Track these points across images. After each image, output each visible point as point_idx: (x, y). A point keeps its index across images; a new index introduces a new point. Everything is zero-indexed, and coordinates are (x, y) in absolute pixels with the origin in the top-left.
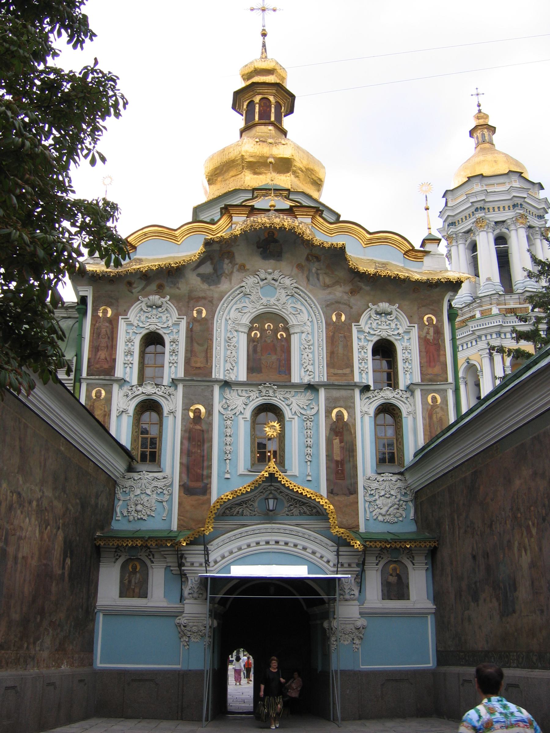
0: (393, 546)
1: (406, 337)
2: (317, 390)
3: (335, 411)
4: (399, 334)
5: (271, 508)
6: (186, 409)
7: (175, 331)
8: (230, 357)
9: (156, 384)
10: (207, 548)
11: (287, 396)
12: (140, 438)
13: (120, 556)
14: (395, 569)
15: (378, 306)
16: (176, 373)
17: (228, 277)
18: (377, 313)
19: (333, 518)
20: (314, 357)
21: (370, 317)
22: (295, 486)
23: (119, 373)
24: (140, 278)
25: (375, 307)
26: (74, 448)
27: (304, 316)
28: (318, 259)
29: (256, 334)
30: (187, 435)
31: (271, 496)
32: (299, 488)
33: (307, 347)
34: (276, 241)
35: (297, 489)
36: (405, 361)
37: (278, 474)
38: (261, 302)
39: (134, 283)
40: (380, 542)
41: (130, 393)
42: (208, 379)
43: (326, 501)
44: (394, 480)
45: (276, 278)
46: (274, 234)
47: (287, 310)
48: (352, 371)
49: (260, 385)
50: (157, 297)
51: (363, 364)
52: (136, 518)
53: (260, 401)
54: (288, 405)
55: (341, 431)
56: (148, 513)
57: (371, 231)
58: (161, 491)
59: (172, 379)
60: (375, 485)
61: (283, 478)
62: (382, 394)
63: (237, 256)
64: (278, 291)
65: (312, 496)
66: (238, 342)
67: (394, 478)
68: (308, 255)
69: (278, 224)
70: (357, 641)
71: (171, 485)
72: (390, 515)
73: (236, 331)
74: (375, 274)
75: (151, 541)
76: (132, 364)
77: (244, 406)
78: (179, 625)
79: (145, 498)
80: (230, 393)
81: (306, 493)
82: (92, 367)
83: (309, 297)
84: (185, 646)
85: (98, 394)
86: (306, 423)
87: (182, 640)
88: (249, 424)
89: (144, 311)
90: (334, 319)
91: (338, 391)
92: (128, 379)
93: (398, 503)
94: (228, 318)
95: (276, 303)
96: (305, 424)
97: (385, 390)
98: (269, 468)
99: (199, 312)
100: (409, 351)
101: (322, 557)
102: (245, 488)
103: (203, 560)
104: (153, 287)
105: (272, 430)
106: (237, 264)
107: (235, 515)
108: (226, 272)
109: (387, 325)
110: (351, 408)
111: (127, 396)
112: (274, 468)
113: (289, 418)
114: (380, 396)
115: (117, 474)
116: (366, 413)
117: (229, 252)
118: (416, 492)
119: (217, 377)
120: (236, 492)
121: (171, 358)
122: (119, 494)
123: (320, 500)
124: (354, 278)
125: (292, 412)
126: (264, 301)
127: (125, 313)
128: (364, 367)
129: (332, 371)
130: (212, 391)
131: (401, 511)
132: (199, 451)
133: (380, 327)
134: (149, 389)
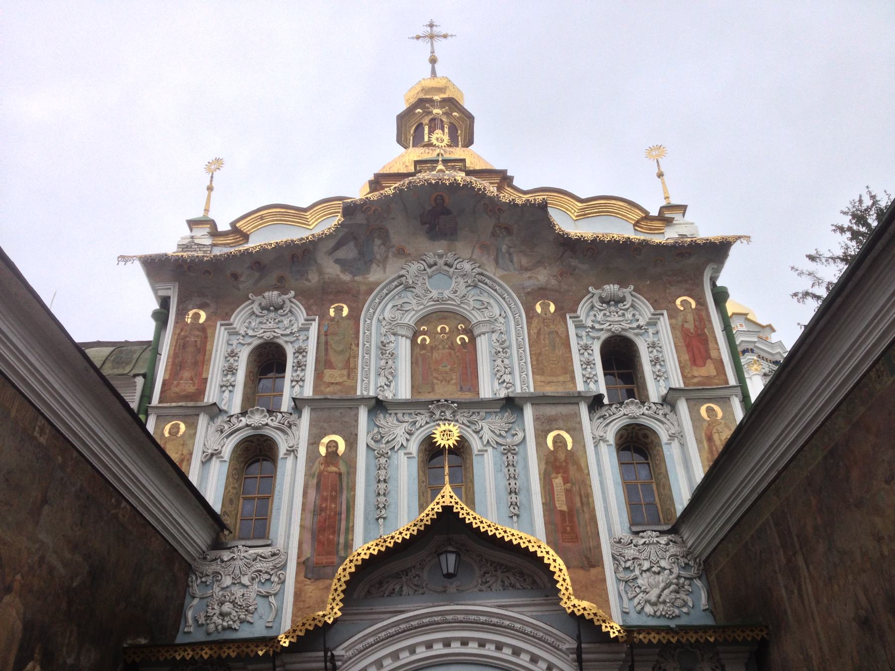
0: (684, 640)
1: (651, 331)
2: (520, 410)
4: (639, 327)
6: (314, 442)
7: (301, 338)
9: (268, 411)
10: (332, 654)
11: (475, 418)
12: (241, 500)
16: (301, 393)
18: (602, 301)
19: (564, 580)
20: (512, 363)
22: (489, 526)
24: (251, 268)
25: (599, 291)
26: (75, 454)
27: (496, 311)
28: (508, 230)
29: (424, 339)
30: (315, 481)
31: (450, 548)
32: (497, 529)
34: (447, 212)
35: (494, 531)
36: (655, 361)
37: (459, 506)
39: (241, 275)
40: (658, 633)
42: (349, 396)
43: (548, 549)
44: (663, 542)
45: (450, 261)
46: (444, 202)
47: (469, 305)
48: (573, 378)
50: (276, 293)
51: (589, 370)
52: (220, 627)
54: (477, 432)
55: (562, 466)
56: (242, 616)
57: (583, 197)
58: (267, 576)
59: (294, 399)
60: (631, 552)
61: (468, 514)
62: (623, 411)
63: (391, 232)
65: (521, 541)
66: (396, 348)
67: (663, 540)
68: (494, 228)
69: (449, 180)
71: (284, 567)
72: (664, 602)
73: (394, 334)
74: (594, 241)
75: (229, 648)
76: (233, 386)
77: (408, 437)
79: (238, 592)
80: (385, 417)
81: (511, 537)
83: (500, 285)
85: (175, 430)
86: (505, 458)
88: (415, 464)
89: (257, 316)
90: (539, 309)
91: (553, 406)
92: (223, 407)
93: (675, 581)
94: (381, 318)
96: (505, 458)
97: (627, 404)
98: (443, 497)
102: (401, 533)
104: (272, 278)
105: (446, 437)
106: (393, 247)
108: (378, 257)
110: (576, 431)
111: (222, 432)
112: (451, 497)
113: (479, 451)
114: (622, 413)
115: (189, 548)
116: (602, 439)
117: (380, 228)
118: (705, 562)
119: (365, 393)
120: (385, 541)
121: (295, 374)
122: (196, 589)
123: (536, 548)
124: (563, 254)
125: (483, 442)
126: (434, 294)
127: (228, 316)
128: (590, 373)
129: (543, 379)
130: (357, 415)
131: (683, 595)
132: (333, 506)
133: (609, 319)
134: (257, 419)
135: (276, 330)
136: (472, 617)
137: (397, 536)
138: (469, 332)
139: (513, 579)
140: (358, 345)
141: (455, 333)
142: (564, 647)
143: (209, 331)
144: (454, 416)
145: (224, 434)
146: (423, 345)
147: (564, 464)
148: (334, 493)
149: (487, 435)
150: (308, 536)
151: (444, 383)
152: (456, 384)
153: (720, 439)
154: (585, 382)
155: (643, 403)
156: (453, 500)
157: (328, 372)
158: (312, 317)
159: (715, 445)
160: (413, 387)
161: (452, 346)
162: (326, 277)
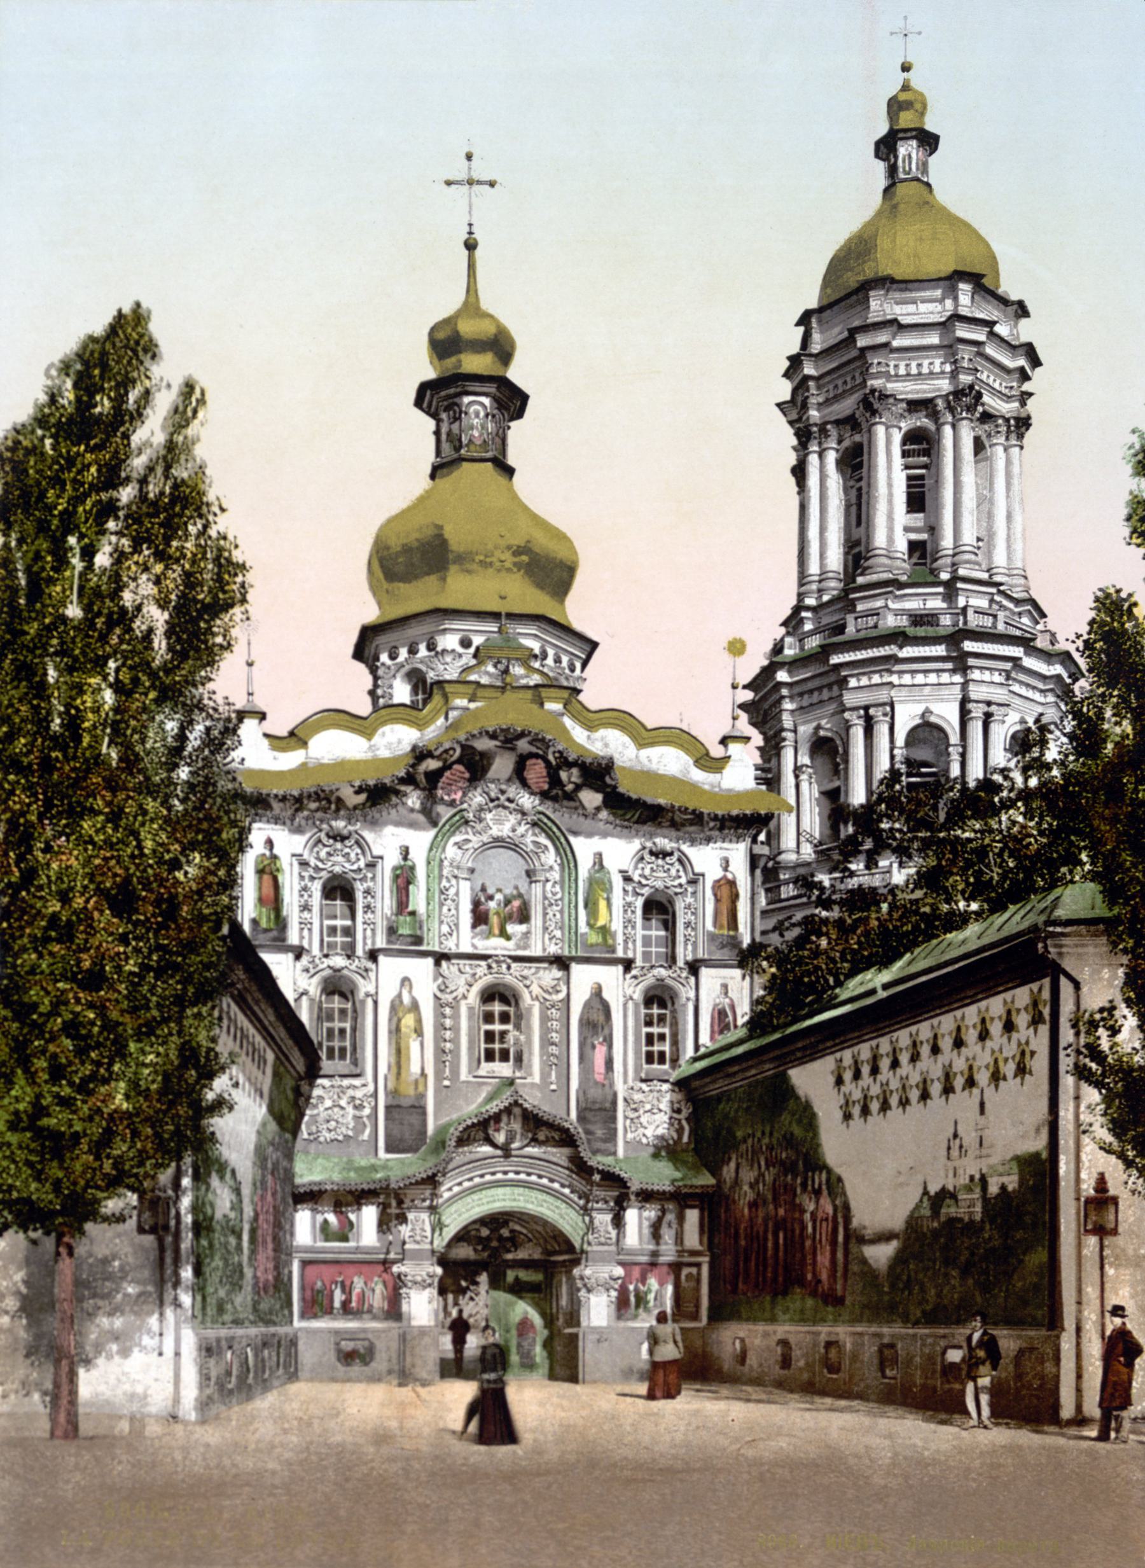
1: (690, 890)
4: (681, 885)
7: (370, 875)
18: (652, 853)
21: (642, 858)
53: (489, 979)
73: (456, 877)
149: (535, 989)
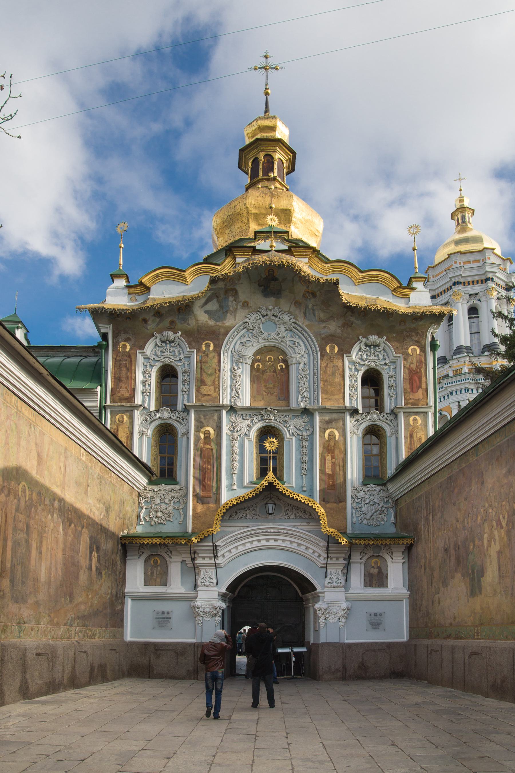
1: (392, 367)
2: (313, 414)
3: (327, 432)
4: (386, 364)
5: (270, 512)
7: (186, 363)
8: (236, 384)
11: (287, 419)
13: (143, 553)
14: (376, 563)
15: (368, 339)
17: (233, 314)
18: (366, 345)
22: (291, 493)
23: (139, 400)
29: (258, 365)
30: (199, 453)
32: (294, 495)
33: (304, 376)
36: (390, 387)
38: (263, 336)
41: (148, 419)
42: (216, 404)
49: (262, 409)
50: (170, 333)
51: (354, 391)
61: (281, 487)
64: (278, 326)
70: (343, 620)
78: (194, 607)
80: (236, 416)
81: (301, 499)
82: (115, 396)
83: (306, 332)
84: (199, 624)
87: (196, 619)
89: (159, 346)
90: (328, 350)
92: (146, 405)
94: (233, 351)
95: (276, 337)
96: (301, 443)
98: (269, 477)
99: (208, 346)
100: (394, 379)
101: (314, 552)
102: (247, 495)
103: (212, 555)
107: (240, 519)
108: (231, 309)
109: (375, 356)
112: (273, 478)
114: (368, 418)
120: (240, 498)
126: (266, 335)
127: (142, 347)
129: (326, 397)
132: (209, 467)
133: (369, 358)
135: (171, 357)
136: (280, 531)
137: (246, 496)
138: (285, 361)
139: (300, 514)
140: (219, 370)
141: (277, 362)
142: (321, 544)
143: (133, 357)
144: (275, 417)
145: (148, 422)
146: (258, 370)
147: (333, 448)
148: (209, 460)
149: (292, 429)
150: (197, 483)
151: (269, 395)
152: (276, 396)
153: (417, 437)
154: (350, 398)
155: (380, 413)
156: (273, 479)
157: (203, 387)
158: (192, 350)
159: (414, 440)
160: (251, 397)
161: (275, 371)
162: (200, 322)
